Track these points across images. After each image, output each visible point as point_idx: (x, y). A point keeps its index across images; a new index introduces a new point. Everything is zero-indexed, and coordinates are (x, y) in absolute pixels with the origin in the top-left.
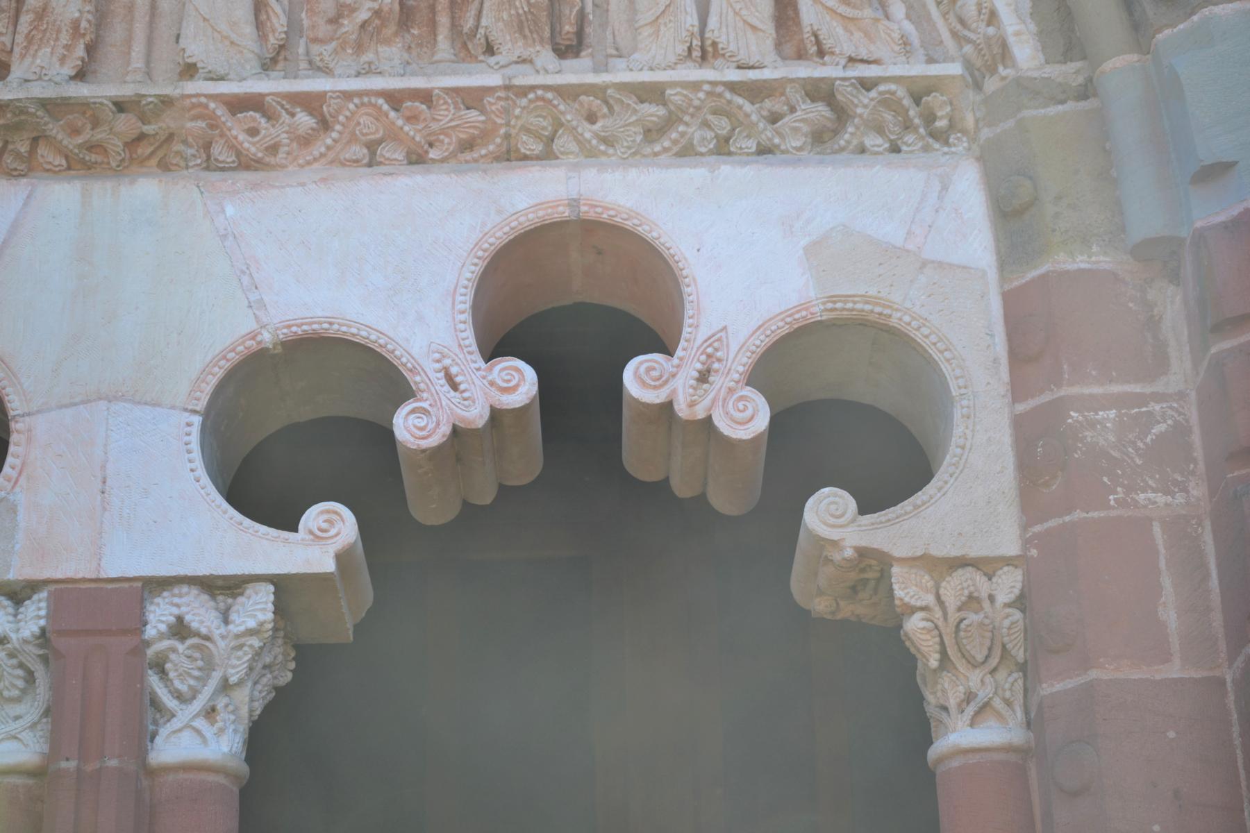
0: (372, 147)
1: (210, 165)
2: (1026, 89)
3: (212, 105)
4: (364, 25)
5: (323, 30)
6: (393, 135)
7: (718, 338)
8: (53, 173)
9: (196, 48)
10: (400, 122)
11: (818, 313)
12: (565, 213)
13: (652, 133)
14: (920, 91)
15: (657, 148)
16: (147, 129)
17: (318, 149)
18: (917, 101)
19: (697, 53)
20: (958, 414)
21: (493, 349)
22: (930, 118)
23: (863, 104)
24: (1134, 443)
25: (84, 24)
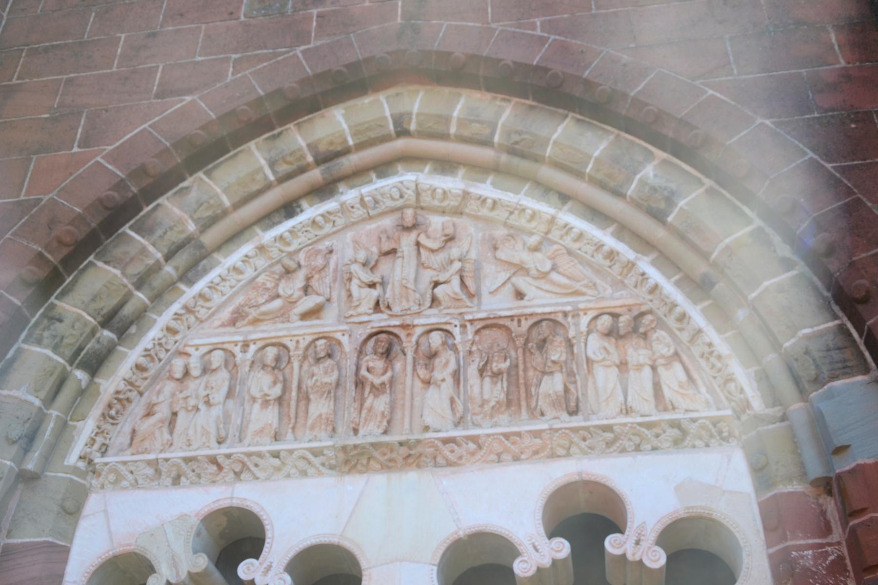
0: (499, 455)
1: (436, 465)
3: (436, 442)
4: (493, 407)
5: (477, 409)
6: (507, 450)
7: (643, 526)
8: (376, 471)
9: (429, 420)
10: (509, 445)
11: (682, 514)
12: (576, 478)
13: (609, 444)
15: (611, 450)
16: (412, 452)
17: (478, 457)
18: (714, 425)
19: (624, 411)
20: (744, 554)
21: (551, 535)
22: (720, 433)
23: (693, 428)
24: (821, 565)
25: (386, 413)
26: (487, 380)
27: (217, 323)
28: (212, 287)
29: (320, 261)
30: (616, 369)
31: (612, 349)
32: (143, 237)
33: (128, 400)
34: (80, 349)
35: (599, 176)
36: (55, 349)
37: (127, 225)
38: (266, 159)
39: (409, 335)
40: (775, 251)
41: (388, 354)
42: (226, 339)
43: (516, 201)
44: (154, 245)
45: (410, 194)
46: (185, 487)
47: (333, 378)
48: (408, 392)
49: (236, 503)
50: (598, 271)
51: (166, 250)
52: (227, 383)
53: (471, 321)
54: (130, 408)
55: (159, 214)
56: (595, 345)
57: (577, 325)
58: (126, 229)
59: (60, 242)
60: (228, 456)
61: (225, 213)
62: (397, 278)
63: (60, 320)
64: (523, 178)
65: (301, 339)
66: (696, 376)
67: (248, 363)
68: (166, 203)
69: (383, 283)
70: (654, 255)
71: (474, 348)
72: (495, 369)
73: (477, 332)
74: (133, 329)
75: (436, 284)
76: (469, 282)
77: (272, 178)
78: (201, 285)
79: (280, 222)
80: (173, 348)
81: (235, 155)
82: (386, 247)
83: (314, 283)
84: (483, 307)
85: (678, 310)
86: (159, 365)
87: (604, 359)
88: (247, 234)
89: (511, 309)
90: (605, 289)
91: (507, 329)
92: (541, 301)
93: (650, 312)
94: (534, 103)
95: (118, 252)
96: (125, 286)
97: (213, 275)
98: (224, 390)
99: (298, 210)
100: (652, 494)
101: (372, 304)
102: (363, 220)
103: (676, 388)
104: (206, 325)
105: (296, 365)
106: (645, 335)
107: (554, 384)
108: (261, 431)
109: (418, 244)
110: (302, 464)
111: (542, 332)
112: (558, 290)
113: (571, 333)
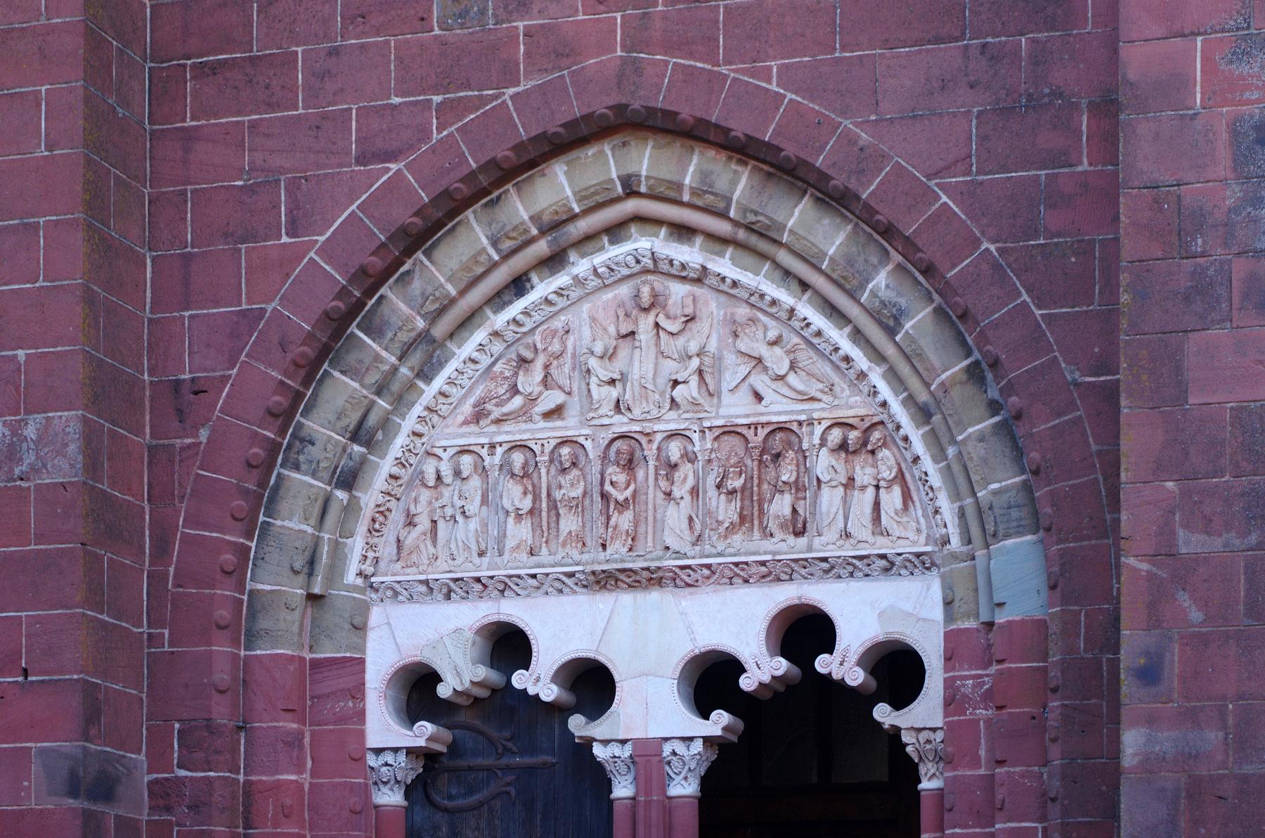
1: (676, 586)
2: (954, 557)
9: (669, 541)
12: (797, 602)
13: (826, 572)
14: (918, 555)
17: (712, 580)
23: (898, 560)
26: (723, 497)
27: (460, 418)
28: (451, 382)
29: (556, 347)
30: (841, 489)
31: (840, 467)
32: (374, 340)
33: (389, 510)
34: (336, 468)
35: (834, 276)
36: (314, 475)
37: (355, 324)
38: (487, 237)
39: (650, 441)
40: (986, 392)
41: (629, 465)
42: (472, 440)
43: (755, 284)
44: (386, 349)
45: (647, 262)
46: (455, 601)
47: (578, 492)
48: (650, 519)
49: (503, 618)
50: (837, 368)
51: (399, 353)
52: (480, 492)
53: (710, 428)
54: (391, 516)
55: (385, 309)
56: (824, 463)
57: (812, 433)
58: (353, 328)
59: (297, 365)
60: (492, 577)
61: (453, 301)
62: (636, 377)
63: (313, 444)
64: (764, 257)
65: (545, 442)
66: (915, 498)
67: (497, 468)
68: (390, 294)
69: (624, 377)
70: (884, 367)
71: (713, 456)
72: (730, 488)
73: (716, 438)
74: (380, 435)
75: (676, 383)
76: (708, 378)
77: (496, 258)
78: (439, 382)
79: (511, 302)
80: (421, 451)
81: (454, 228)
82: (624, 331)
83: (553, 371)
84: (722, 411)
85: (902, 432)
86: (410, 470)
87: (831, 480)
88: (477, 320)
89: (747, 416)
90: (843, 390)
91: (744, 436)
92: (779, 408)
93: (882, 423)
94: (772, 170)
95: (351, 358)
96: (366, 397)
97: (448, 370)
98: (478, 499)
99: (528, 285)
100: (862, 617)
101: (612, 404)
102: (598, 289)
103: (892, 514)
104: (449, 421)
105: (543, 471)
106: (873, 452)
107: (781, 506)
108: (518, 547)
109: (657, 325)
110: (557, 584)
111: (779, 441)
112: (793, 395)
113: (805, 446)
